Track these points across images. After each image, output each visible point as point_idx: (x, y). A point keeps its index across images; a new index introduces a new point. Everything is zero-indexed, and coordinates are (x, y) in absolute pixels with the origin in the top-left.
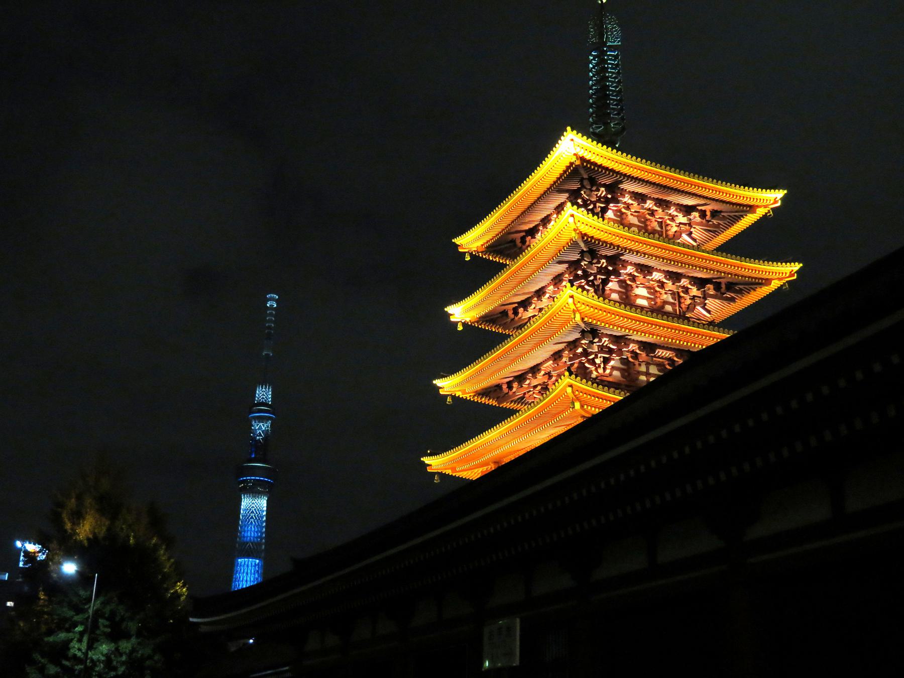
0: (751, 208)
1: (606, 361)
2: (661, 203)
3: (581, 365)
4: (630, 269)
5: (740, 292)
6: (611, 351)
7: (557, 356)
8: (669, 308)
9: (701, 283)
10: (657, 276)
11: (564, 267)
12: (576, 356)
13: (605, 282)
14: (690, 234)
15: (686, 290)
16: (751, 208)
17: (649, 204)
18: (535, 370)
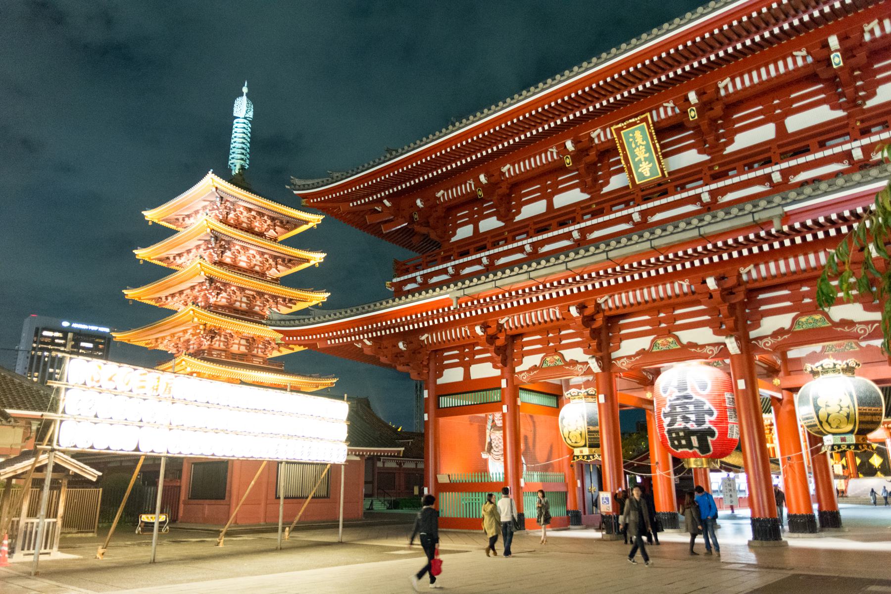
0: (307, 222)
1: (218, 294)
2: (259, 213)
3: (205, 295)
4: (237, 247)
5: (294, 264)
6: (221, 290)
7: (192, 288)
8: (257, 268)
9: (275, 258)
10: (251, 252)
11: (202, 242)
12: (202, 290)
13: (223, 253)
14: (275, 230)
15: (267, 261)
16: (307, 222)
17: (253, 213)
18: (181, 292)
